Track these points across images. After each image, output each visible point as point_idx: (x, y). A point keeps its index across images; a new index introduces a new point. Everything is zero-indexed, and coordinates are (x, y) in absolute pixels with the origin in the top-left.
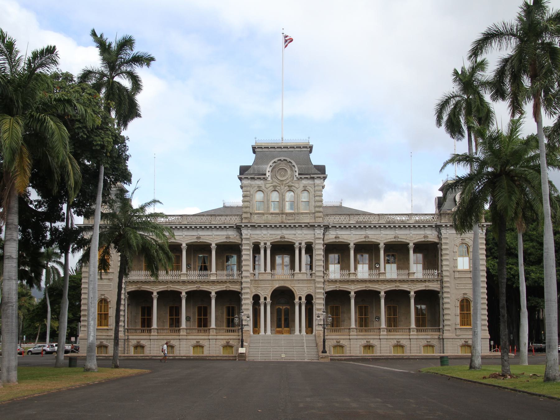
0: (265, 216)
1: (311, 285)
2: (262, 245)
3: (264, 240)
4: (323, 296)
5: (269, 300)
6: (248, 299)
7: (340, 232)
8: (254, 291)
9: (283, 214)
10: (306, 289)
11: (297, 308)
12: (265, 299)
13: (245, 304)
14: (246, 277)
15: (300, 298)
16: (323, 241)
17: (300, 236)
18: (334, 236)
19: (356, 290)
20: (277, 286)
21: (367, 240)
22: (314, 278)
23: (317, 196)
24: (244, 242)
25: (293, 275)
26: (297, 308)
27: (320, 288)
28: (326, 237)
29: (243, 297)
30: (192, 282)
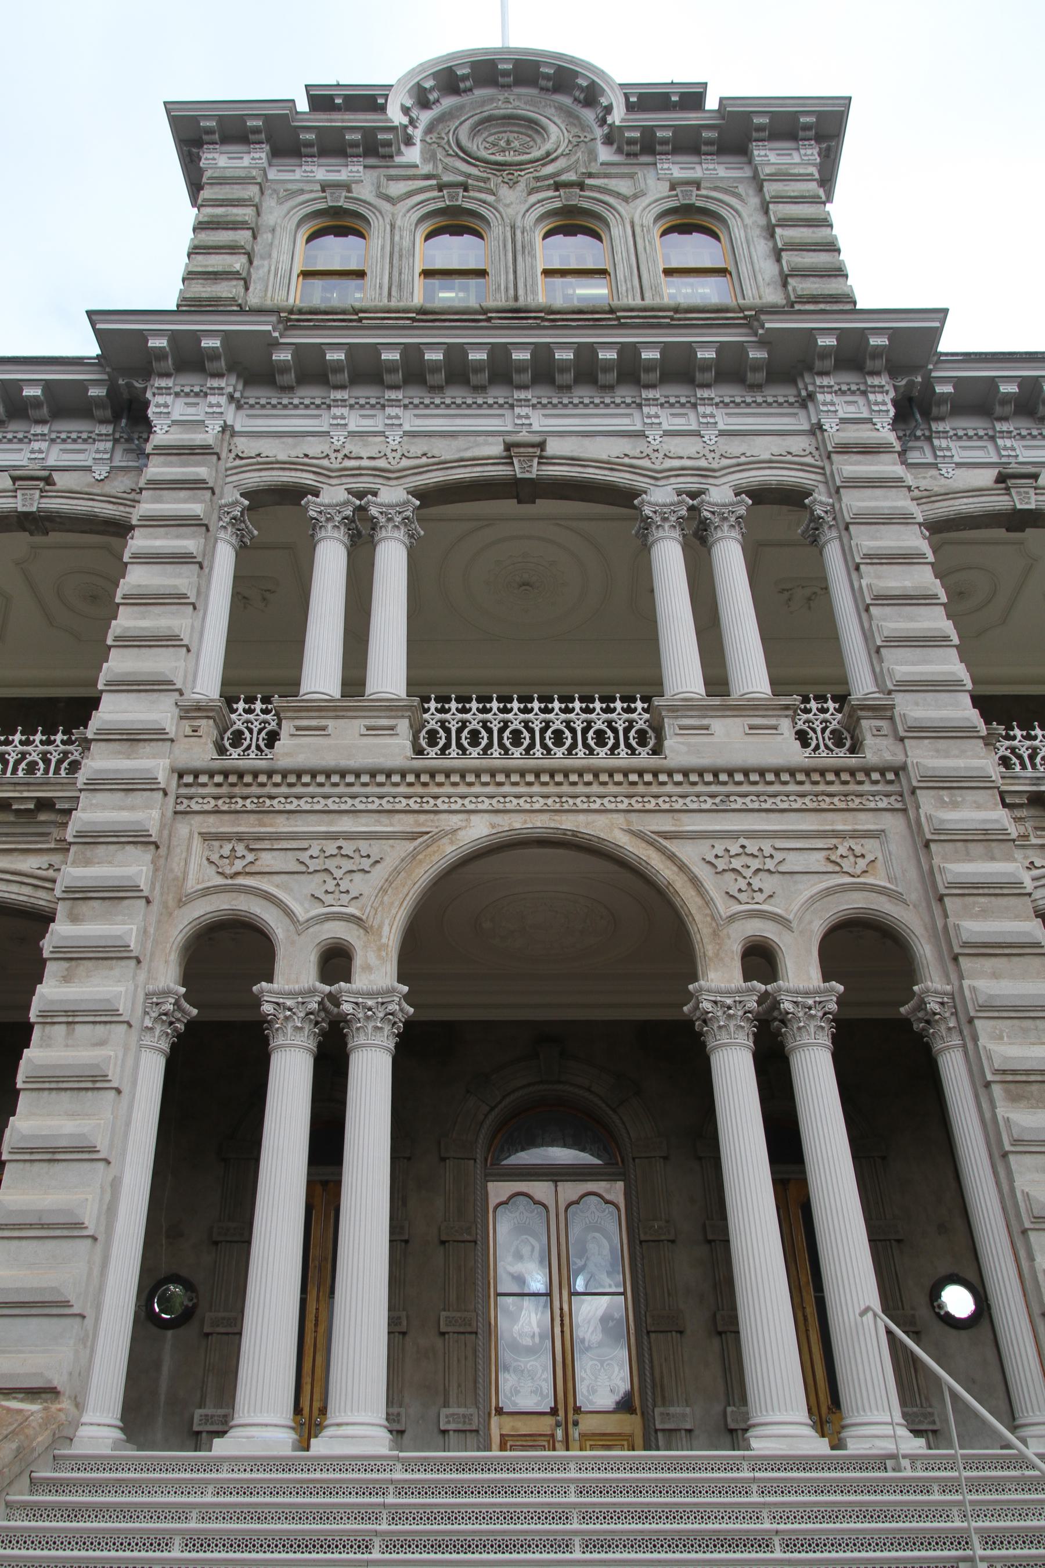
1: (866, 822)
3: (357, 472)
5: (376, 972)
6: (109, 954)
8: (197, 869)
10: (816, 861)
11: (735, 1073)
12: (336, 962)
13: (71, 1017)
14: (132, 738)
15: (760, 960)
17: (675, 445)
20: (478, 830)
22: (877, 748)
25: (652, 737)
26: (735, 1073)
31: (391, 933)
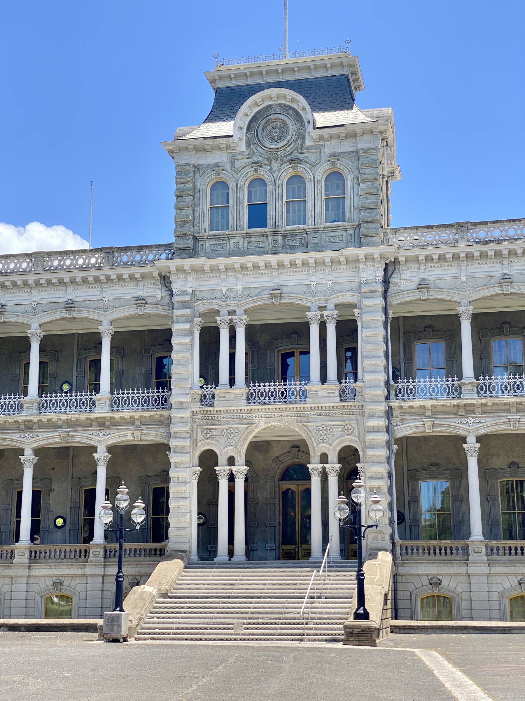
0: (232, 241)
2: (223, 320)
4: (383, 453)
7: (433, 273)
9: (275, 233)
12: (231, 461)
15: (324, 459)
16: (385, 298)
18: (415, 285)
19: (482, 432)
20: (262, 425)
21: (507, 289)
23: (364, 181)
24: (177, 312)
27: (378, 430)
28: (392, 289)
29: (173, 459)
30: (51, 425)
31: (243, 453)
